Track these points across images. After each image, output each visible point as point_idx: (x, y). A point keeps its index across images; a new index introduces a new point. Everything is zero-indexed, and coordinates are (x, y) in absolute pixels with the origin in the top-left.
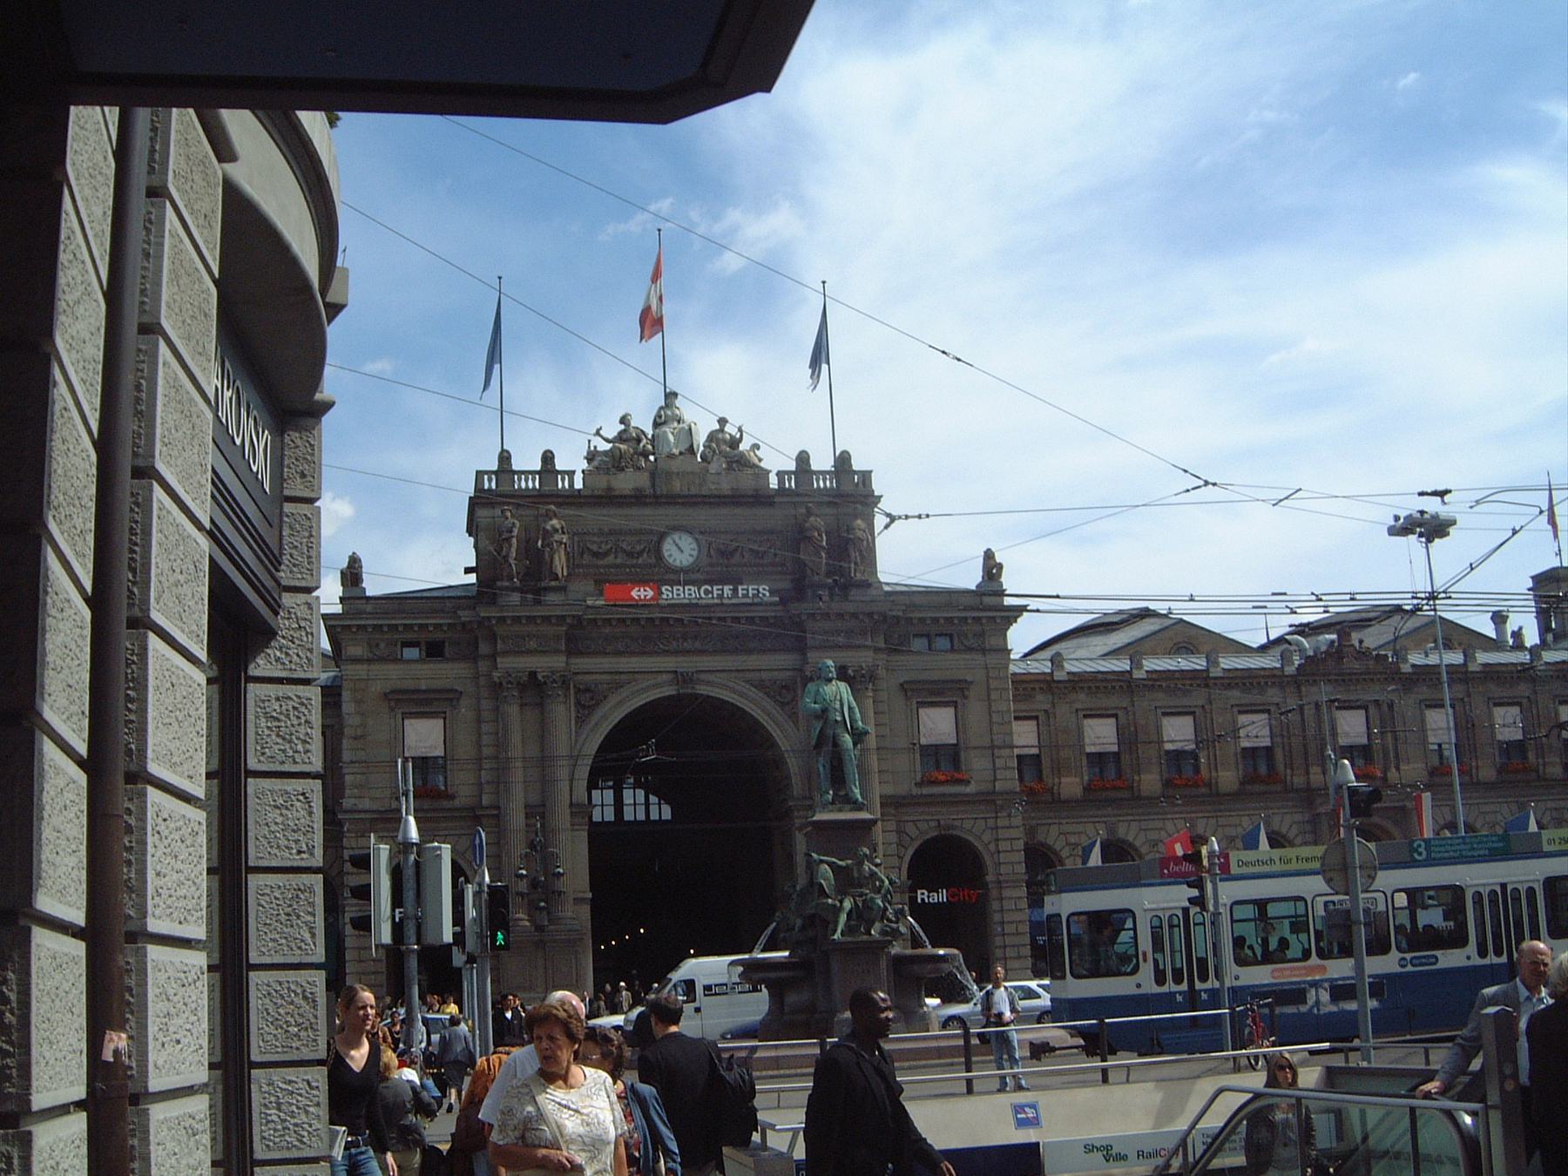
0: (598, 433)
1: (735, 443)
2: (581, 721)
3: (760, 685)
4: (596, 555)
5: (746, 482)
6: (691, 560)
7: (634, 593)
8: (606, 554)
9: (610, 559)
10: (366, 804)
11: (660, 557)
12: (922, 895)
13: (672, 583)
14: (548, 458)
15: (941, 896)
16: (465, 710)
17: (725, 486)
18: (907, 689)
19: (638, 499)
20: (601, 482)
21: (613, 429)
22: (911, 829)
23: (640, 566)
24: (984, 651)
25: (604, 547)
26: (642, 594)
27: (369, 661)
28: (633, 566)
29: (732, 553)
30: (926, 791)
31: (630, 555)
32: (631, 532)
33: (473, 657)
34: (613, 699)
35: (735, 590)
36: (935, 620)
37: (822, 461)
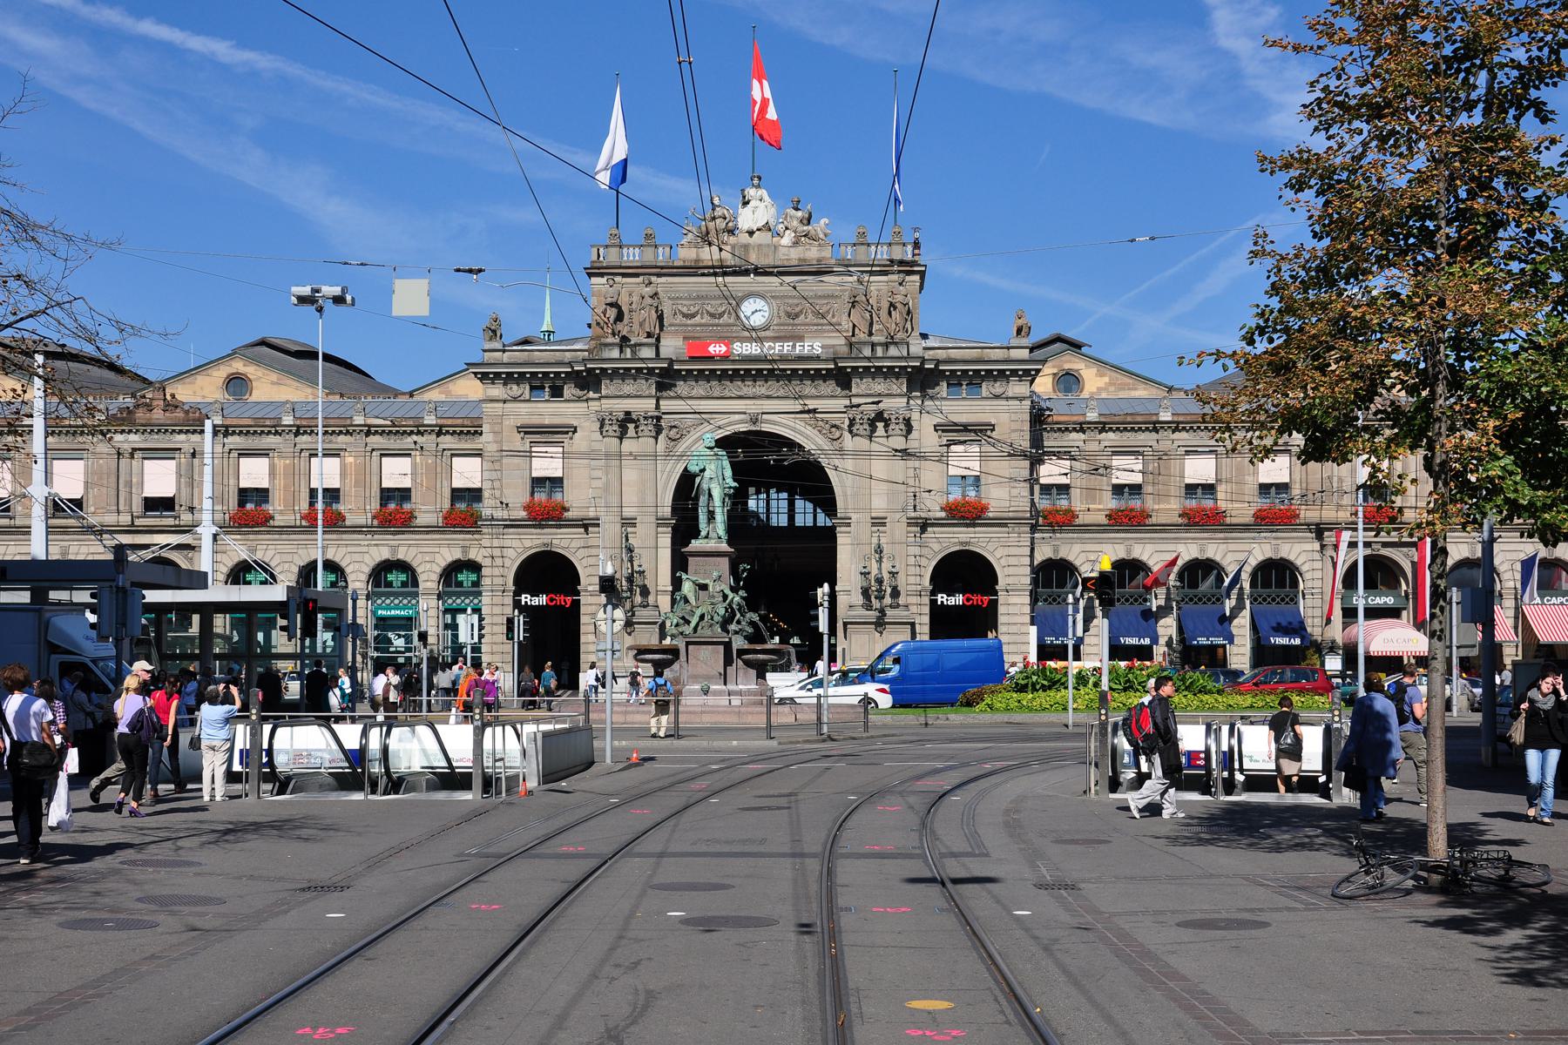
4: (685, 316)
5: (812, 253)
7: (711, 349)
8: (693, 316)
9: (697, 319)
11: (738, 317)
12: (942, 598)
13: (742, 340)
15: (958, 600)
17: (794, 255)
19: (721, 270)
24: (1007, 398)
25: (693, 310)
29: (797, 316)
31: (712, 315)
35: (794, 347)
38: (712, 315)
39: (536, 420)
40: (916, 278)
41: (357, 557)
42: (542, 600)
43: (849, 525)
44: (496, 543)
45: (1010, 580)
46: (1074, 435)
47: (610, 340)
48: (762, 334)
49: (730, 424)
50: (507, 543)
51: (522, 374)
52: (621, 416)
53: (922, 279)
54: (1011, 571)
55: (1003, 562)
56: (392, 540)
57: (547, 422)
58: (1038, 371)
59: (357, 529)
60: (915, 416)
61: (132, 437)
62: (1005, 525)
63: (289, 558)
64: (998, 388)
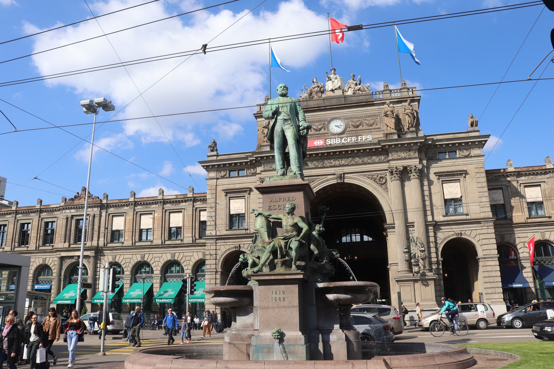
10: (214, 233)
24: (471, 157)
27: (217, 179)
28: (318, 134)
29: (358, 126)
32: (317, 122)
33: (254, 174)
35: (357, 140)
38: (316, 130)
40: (416, 103)
41: (157, 259)
43: (394, 228)
47: (266, 144)
48: (342, 136)
49: (327, 180)
50: (218, 247)
53: (419, 103)
54: (485, 247)
56: (173, 250)
57: (237, 186)
58: (486, 141)
59: (157, 247)
61: (73, 211)
62: (479, 223)
63: (128, 260)
64: (466, 153)
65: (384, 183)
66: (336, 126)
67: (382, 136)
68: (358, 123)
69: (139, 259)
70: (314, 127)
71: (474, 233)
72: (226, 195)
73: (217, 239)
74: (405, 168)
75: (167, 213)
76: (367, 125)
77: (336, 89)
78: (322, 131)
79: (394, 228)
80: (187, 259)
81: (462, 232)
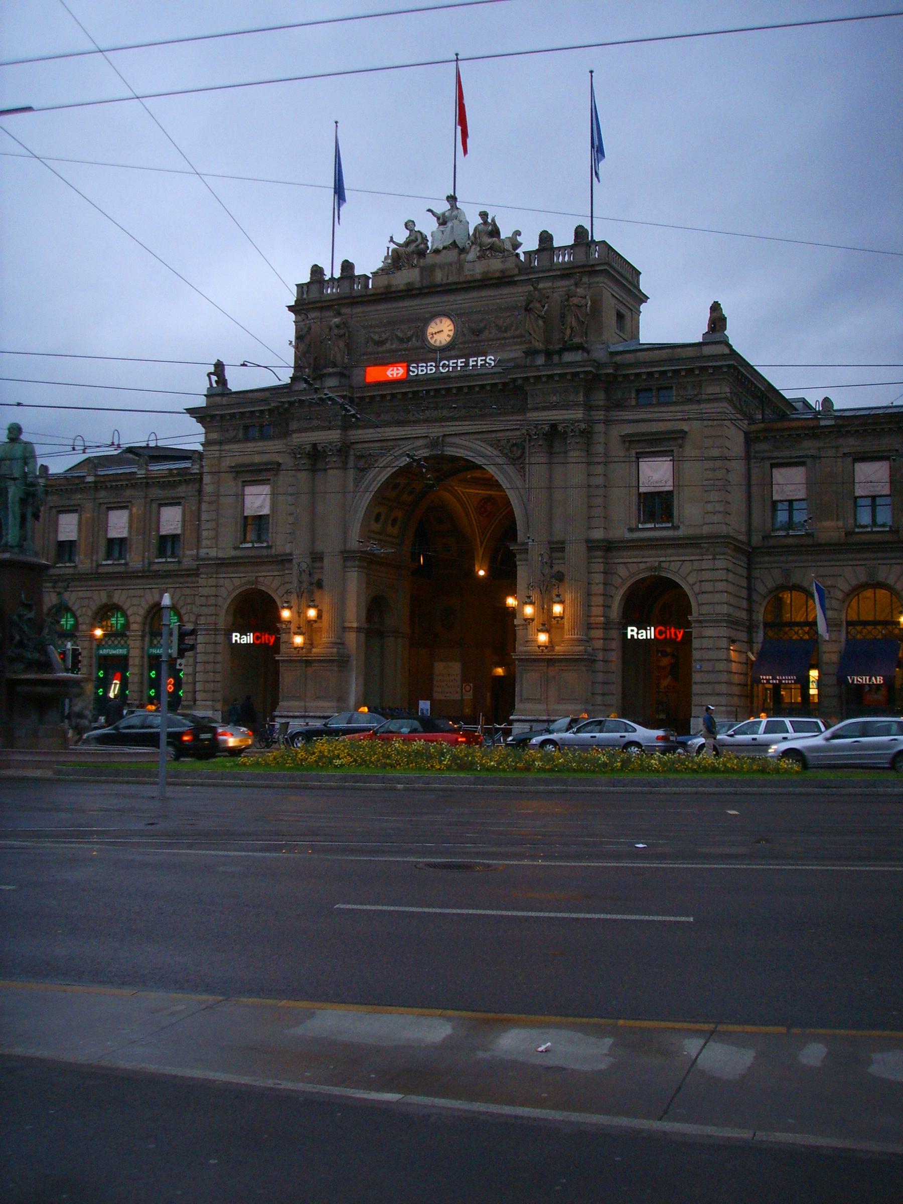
0: (392, 240)
1: (495, 232)
2: (357, 482)
3: (496, 444)
5: (495, 265)
6: (448, 339)
9: (388, 346)
10: (213, 553)
14: (347, 266)
16: (284, 478)
17: (478, 270)
18: (629, 440)
19: (410, 292)
20: (384, 281)
21: (402, 236)
22: (622, 571)
23: (409, 350)
24: (699, 402)
25: (384, 336)
26: (395, 373)
27: (221, 443)
29: (480, 332)
30: (636, 535)
31: (401, 340)
34: (382, 462)
36: (650, 374)
37: (563, 238)
39: (246, 460)
41: (135, 601)
42: (249, 639)
44: (212, 582)
45: (705, 609)
46: (807, 444)
50: (221, 582)
51: (233, 415)
52: (308, 448)
54: (704, 598)
55: (696, 588)
60: (600, 428)
62: (697, 546)
65: (519, 458)
66: (441, 331)
67: (519, 354)
68: (482, 325)
69: (104, 600)
70: (400, 334)
71: (688, 567)
72: (235, 479)
73: (219, 565)
74: (554, 426)
75: (155, 506)
76: (499, 328)
77: (444, 248)
78: (414, 343)
79: (526, 551)
80: (189, 601)
81: (663, 565)
